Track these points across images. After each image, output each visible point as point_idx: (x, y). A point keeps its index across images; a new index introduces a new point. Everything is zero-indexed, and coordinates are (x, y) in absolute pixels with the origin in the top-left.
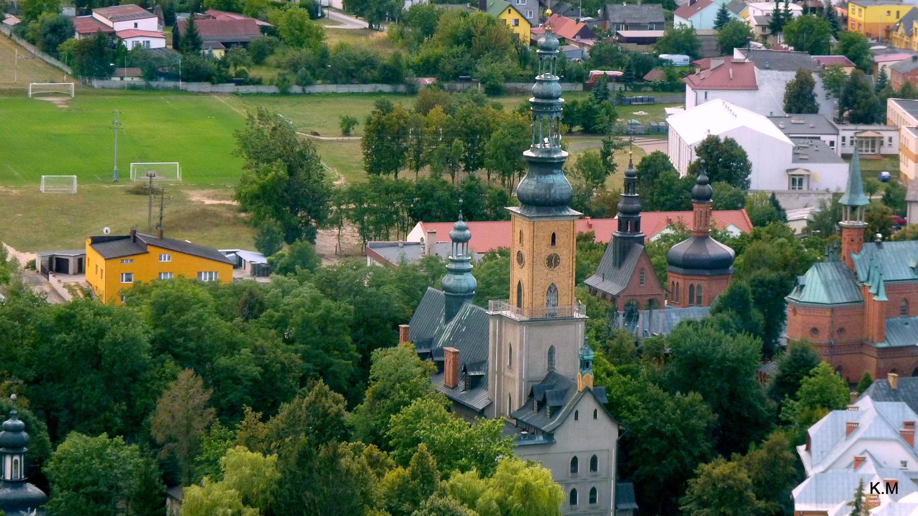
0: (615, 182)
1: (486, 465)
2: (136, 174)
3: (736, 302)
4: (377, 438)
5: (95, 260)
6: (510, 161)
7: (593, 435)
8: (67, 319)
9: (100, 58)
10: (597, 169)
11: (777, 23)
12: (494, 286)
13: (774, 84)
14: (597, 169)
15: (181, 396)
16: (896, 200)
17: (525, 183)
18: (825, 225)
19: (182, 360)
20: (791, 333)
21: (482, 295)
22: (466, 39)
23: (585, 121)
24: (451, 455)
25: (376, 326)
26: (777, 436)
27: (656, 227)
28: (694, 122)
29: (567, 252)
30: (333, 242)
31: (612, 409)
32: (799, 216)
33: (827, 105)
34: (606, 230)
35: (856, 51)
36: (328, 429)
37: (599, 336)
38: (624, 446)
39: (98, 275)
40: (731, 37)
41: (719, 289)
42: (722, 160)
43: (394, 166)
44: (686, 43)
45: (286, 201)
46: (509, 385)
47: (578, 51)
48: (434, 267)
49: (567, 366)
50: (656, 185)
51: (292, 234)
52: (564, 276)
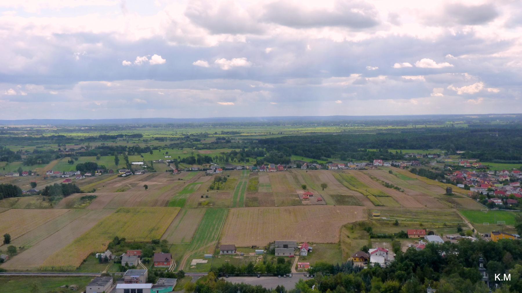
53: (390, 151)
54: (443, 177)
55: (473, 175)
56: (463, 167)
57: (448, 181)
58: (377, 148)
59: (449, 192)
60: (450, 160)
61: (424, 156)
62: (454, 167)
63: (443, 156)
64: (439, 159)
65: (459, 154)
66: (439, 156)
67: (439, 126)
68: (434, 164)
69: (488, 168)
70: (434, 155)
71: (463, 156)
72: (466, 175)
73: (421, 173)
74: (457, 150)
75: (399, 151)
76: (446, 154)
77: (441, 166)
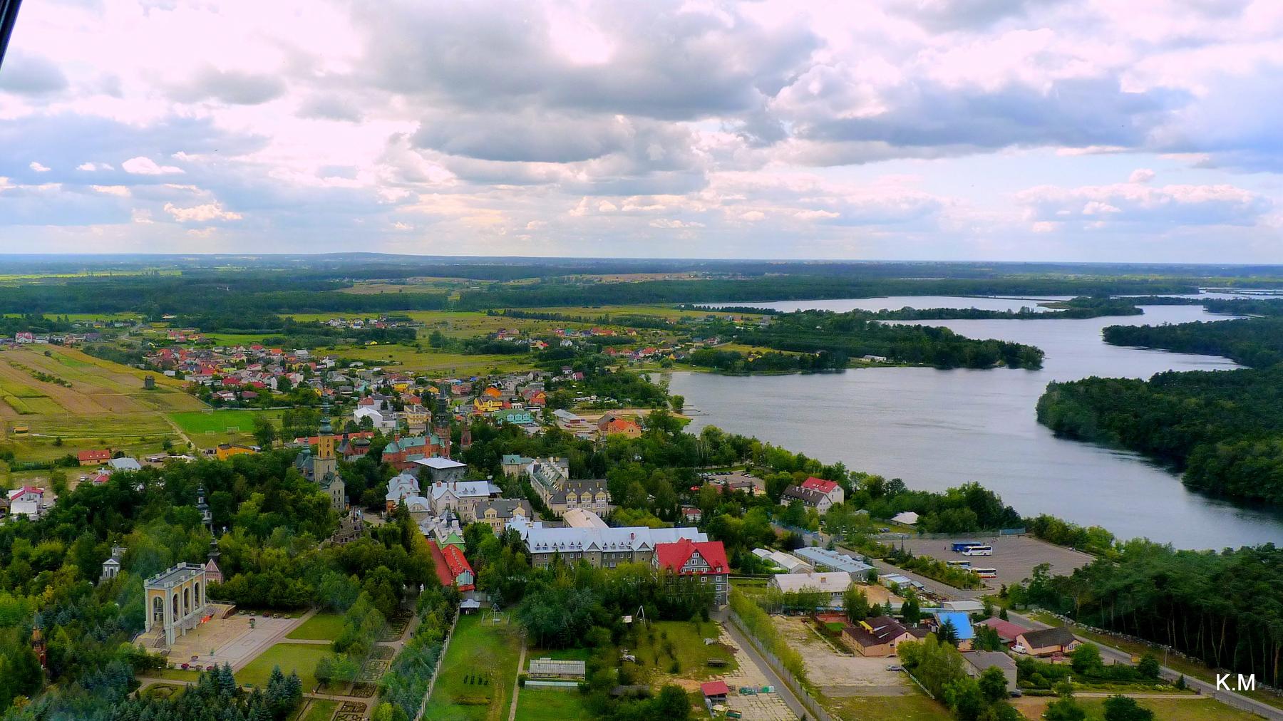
0: (342, 427)
1: (313, 494)
2: (229, 429)
3: (370, 453)
4: (287, 488)
5: (219, 450)
6: (319, 423)
7: (339, 486)
8: (212, 465)
9: (219, 403)
10: (338, 424)
11: (378, 389)
12: (314, 452)
13: (378, 403)
14: (338, 424)
15: (240, 481)
16: (407, 429)
17: (321, 428)
18: (390, 435)
19: (241, 472)
20: (383, 460)
21: (311, 455)
22: (305, 395)
23: (335, 413)
24: (305, 491)
25: (287, 460)
26: (382, 484)
27: (353, 438)
28: (360, 412)
29: (331, 443)
30: (276, 444)
31: (343, 479)
32: (385, 433)
33: (390, 407)
34: (340, 438)
35: (397, 394)
36: (276, 487)
37: (339, 462)
38: (346, 488)
39: (222, 455)
40: (368, 392)
41: (366, 450)
42: (367, 421)
43: (290, 425)
44: (357, 394)
45: (264, 435)
46: (319, 475)
47: (332, 398)
48: (301, 448)
49: (332, 470)
50: (352, 427)
51: (266, 442)
52: (331, 449)
53: (46, 316)
54: (141, 361)
55: (191, 354)
56: (173, 342)
57: (149, 367)
58: (22, 312)
59: (149, 383)
60: (151, 331)
61: (108, 325)
62: (158, 342)
63: (140, 324)
64: (133, 330)
65: (168, 320)
66: (133, 324)
67: (134, 274)
68: (124, 338)
69: (213, 343)
70: (125, 322)
71: (174, 324)
72: (177, 355)
73: (102, 354)
74: (164, 313)
75: (62, 317)
76: (145, 321)
77: (137, 342)
